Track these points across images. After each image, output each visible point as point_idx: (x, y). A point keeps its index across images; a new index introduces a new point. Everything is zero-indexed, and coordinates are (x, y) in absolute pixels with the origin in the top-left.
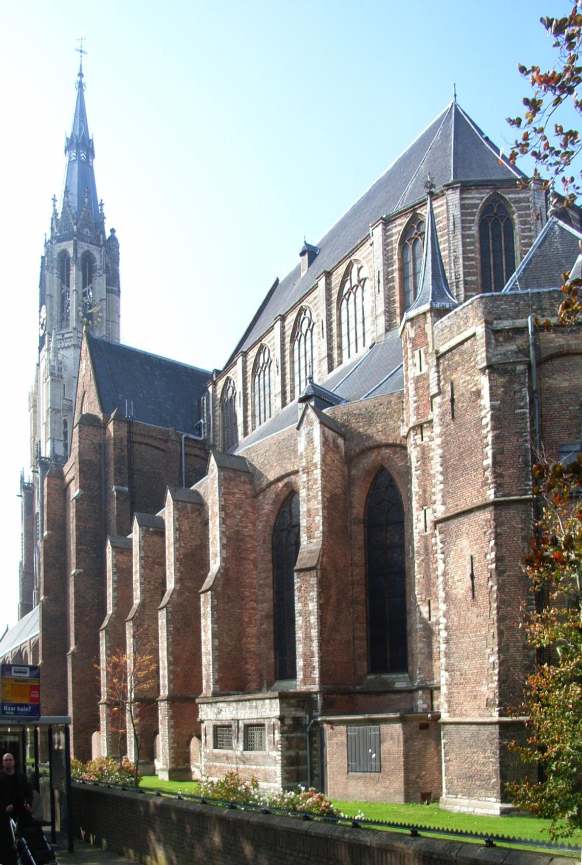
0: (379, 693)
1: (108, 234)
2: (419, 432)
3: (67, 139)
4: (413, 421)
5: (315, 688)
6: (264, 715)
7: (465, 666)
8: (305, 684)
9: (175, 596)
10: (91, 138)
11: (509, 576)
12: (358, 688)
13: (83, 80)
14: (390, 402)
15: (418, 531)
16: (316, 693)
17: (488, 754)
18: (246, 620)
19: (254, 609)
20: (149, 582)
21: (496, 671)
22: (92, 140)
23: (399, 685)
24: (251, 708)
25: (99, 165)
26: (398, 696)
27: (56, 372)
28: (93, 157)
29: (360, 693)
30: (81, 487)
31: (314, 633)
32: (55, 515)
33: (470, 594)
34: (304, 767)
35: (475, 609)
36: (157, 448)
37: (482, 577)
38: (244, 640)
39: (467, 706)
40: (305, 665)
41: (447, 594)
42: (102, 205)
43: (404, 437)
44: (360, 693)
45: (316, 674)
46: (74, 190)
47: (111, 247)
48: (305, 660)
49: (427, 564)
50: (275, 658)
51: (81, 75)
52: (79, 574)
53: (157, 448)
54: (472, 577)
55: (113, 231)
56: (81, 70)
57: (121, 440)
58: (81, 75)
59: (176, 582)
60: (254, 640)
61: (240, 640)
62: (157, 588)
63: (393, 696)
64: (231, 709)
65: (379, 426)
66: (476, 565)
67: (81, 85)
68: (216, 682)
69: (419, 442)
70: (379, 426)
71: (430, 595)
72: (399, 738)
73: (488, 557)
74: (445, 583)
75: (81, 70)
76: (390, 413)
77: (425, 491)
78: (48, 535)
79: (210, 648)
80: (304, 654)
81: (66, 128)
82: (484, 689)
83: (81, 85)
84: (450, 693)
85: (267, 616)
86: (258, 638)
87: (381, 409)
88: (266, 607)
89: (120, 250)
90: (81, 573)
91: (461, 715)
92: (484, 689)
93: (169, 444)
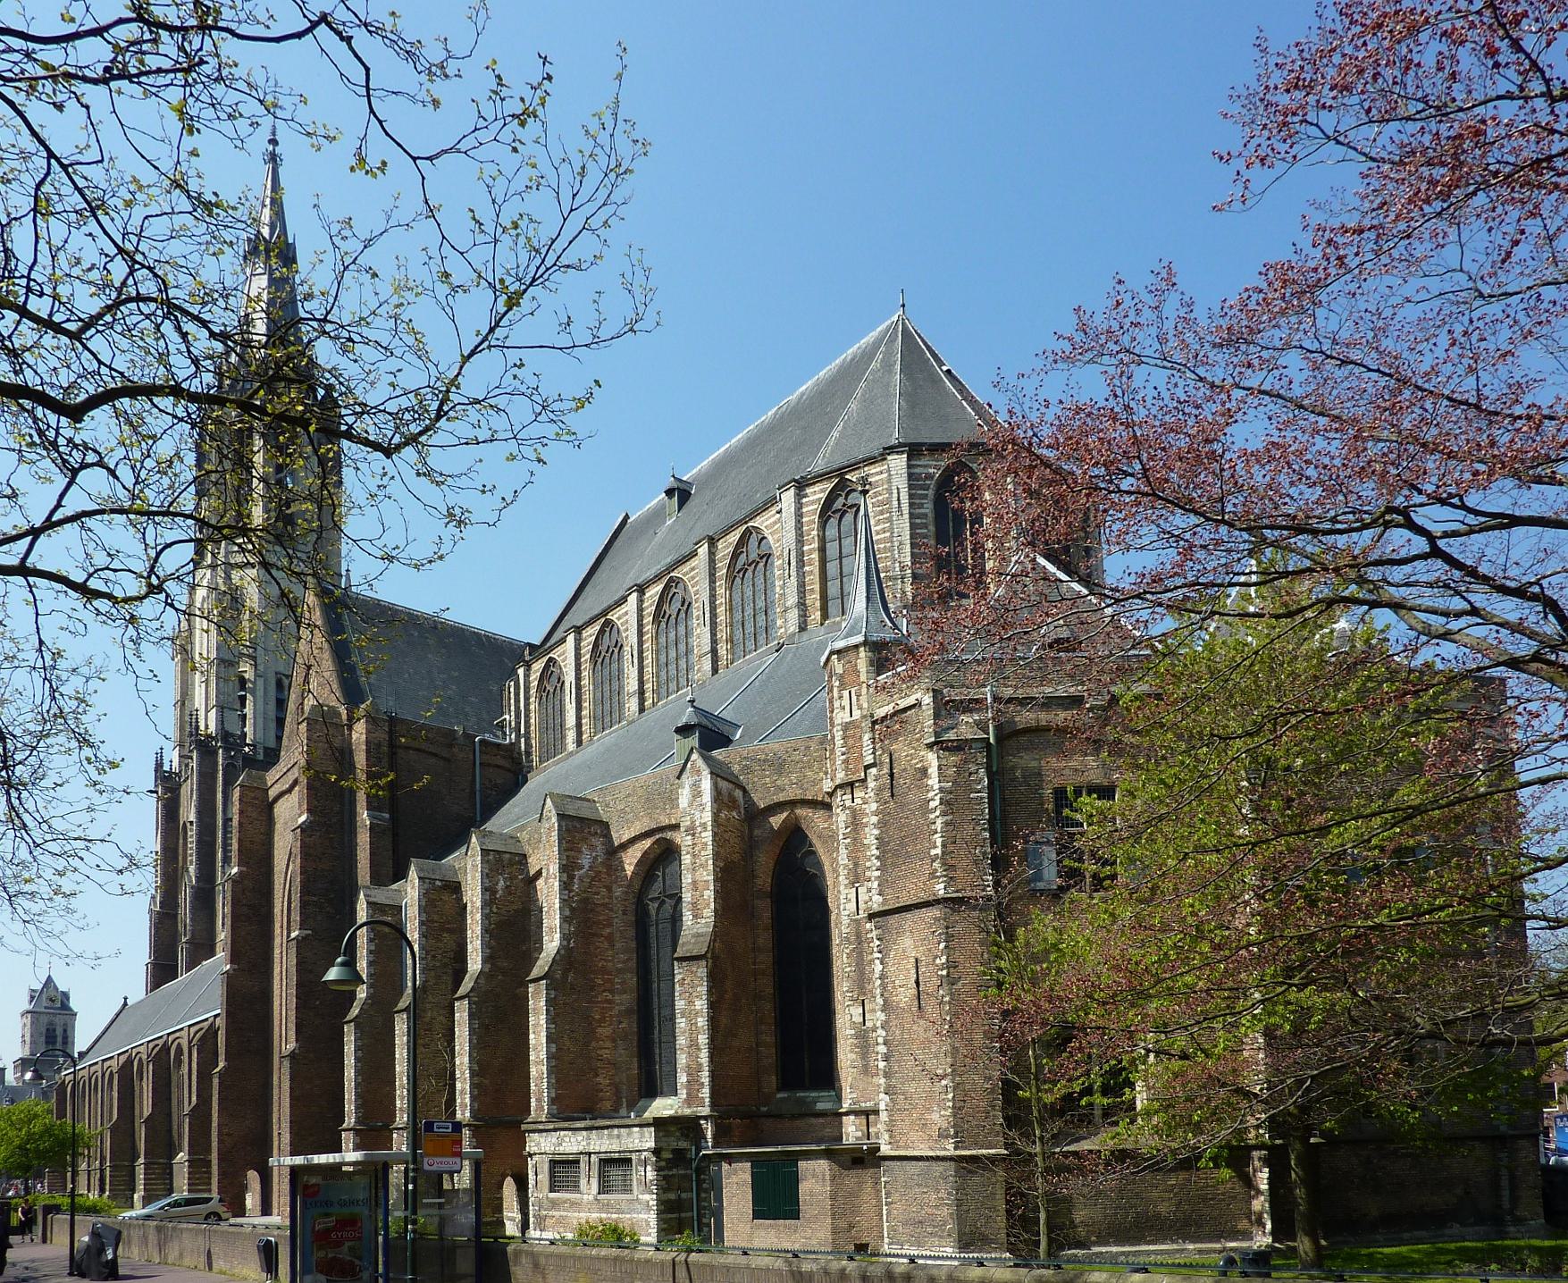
0: (793, 1117)
2: (849, 791)
4: (841, 776)
5: (706, 1111)
6: (631, 1147)
7: (911, 1088)
8: (689, 1107)
9: (482, 981)
10: (290, 241)
11: (964, 985)
12: (764, 1109)
13: (278, 150)
14: (808, 748)
15: (847, 913)
16: (705, 1118)
17: (943, 1194)
18: (597, 1017)
19: (609, 1001)
20: (434, 956)
21: (950, 1096)
23: (820, 1106)
24: (610, 1137)
26: (821, 1120)
29: (768, 1115)
30: (309, 810)
31: (703, 1039)
32: (252, 842)
33: (916, 1003)
34: (689, 1214)
35: (922, 1022)
36: (435, 755)
37: (930, 984)
38: (594, 1044)
39: (914, 1136)
40: (688, 1081)
41: (885, 1001)
43: (828, 793)
44: (768, 1115)
45: (706, 1092)
48: (688, 1075)
49: (860, 954)
50: (640, 1067)
52: (305, 938)
53: (435, 755)
54: (917, 982)
56: (274, 133)
57: (379, 745)
58: (274, 142)
59: (484, 961)
60: (608, 1044)
61: (587, 1044)
62: (445, 965)
63: (813, 1121)
64: (580, 1138)
65: (793, 777)
66: (922, 970)
68: (552, 1101)
69: (848, 803)
70: (793, 777)
71: (864, 994)
72: (824, 1175)
73: (938, 961)
74: (884, 987)
75: (274, 133)
76: (809, 761)
77: (856, 865)
78: (240, 873)
79: (543, 1055)
80: (688, 1067)
82: (935, 1116)
83: (273, 159)
84: (891, 1121)
85: (628, 1012)
86: (614, 1041)
87: (796, 756)
88: (625, 999)
90: (308, 935)
91: (907, 1147)
92: (935, 1116)
93: (455, 750)
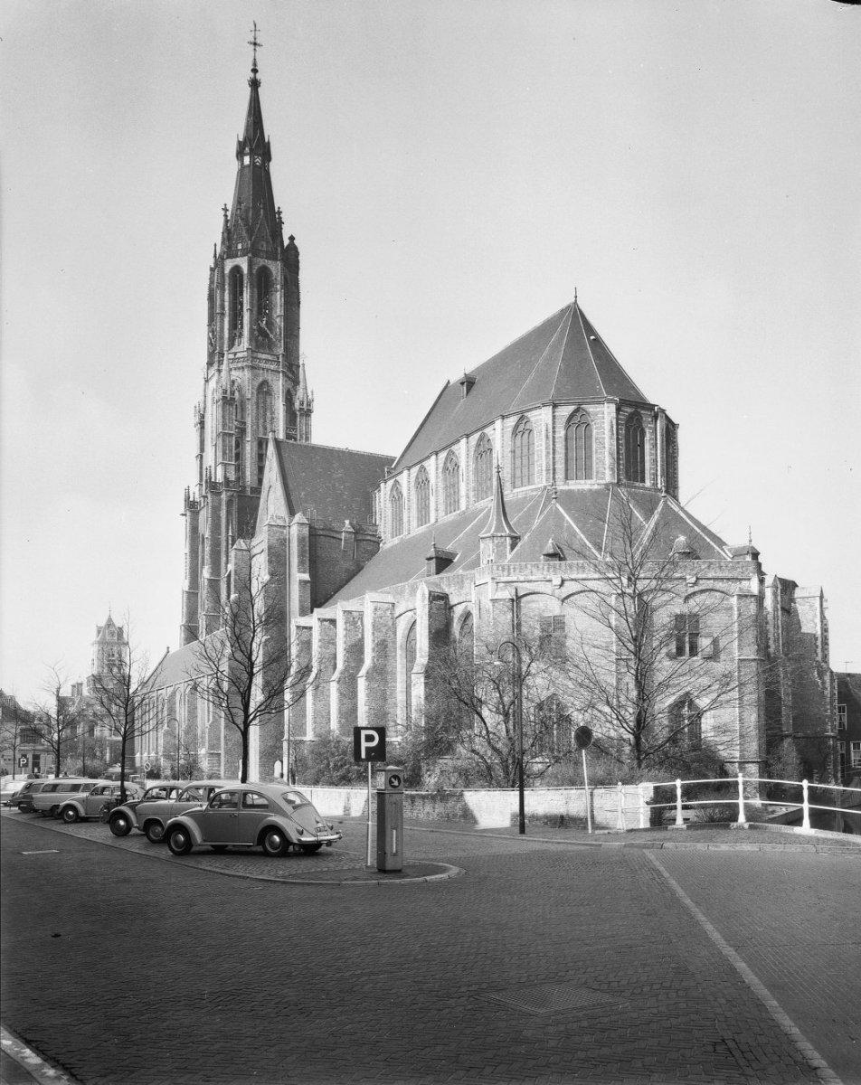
1: (286, 242)
3: (239, 142)
13: (258, 76)
22: (269, 143)
25: (279, 171)
27: (228, 395)
28: (270, 159)
42: (280, 213)
46: (248, 203)
47: (290, 258)
51: (255, 71)
55: (292, 238)
58: (255, 71)
67: (255, 84)
81: (239, 129)
83: (255, 84)
89: (300, 258)
